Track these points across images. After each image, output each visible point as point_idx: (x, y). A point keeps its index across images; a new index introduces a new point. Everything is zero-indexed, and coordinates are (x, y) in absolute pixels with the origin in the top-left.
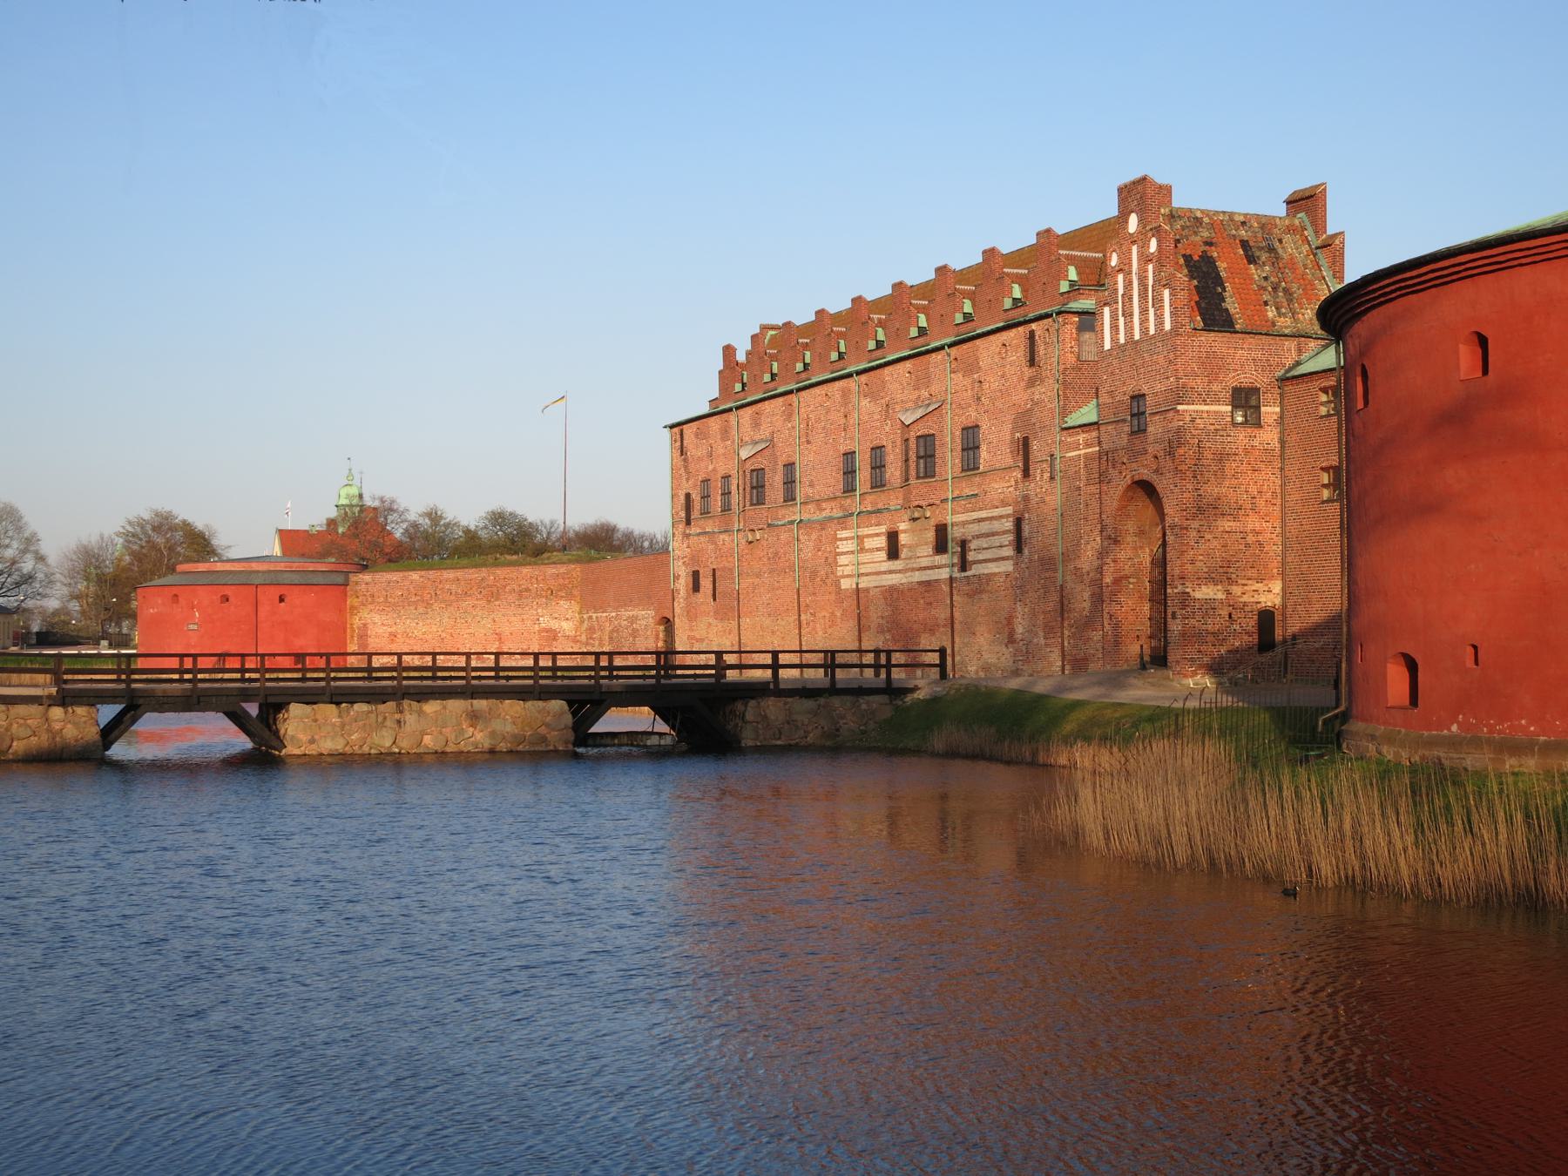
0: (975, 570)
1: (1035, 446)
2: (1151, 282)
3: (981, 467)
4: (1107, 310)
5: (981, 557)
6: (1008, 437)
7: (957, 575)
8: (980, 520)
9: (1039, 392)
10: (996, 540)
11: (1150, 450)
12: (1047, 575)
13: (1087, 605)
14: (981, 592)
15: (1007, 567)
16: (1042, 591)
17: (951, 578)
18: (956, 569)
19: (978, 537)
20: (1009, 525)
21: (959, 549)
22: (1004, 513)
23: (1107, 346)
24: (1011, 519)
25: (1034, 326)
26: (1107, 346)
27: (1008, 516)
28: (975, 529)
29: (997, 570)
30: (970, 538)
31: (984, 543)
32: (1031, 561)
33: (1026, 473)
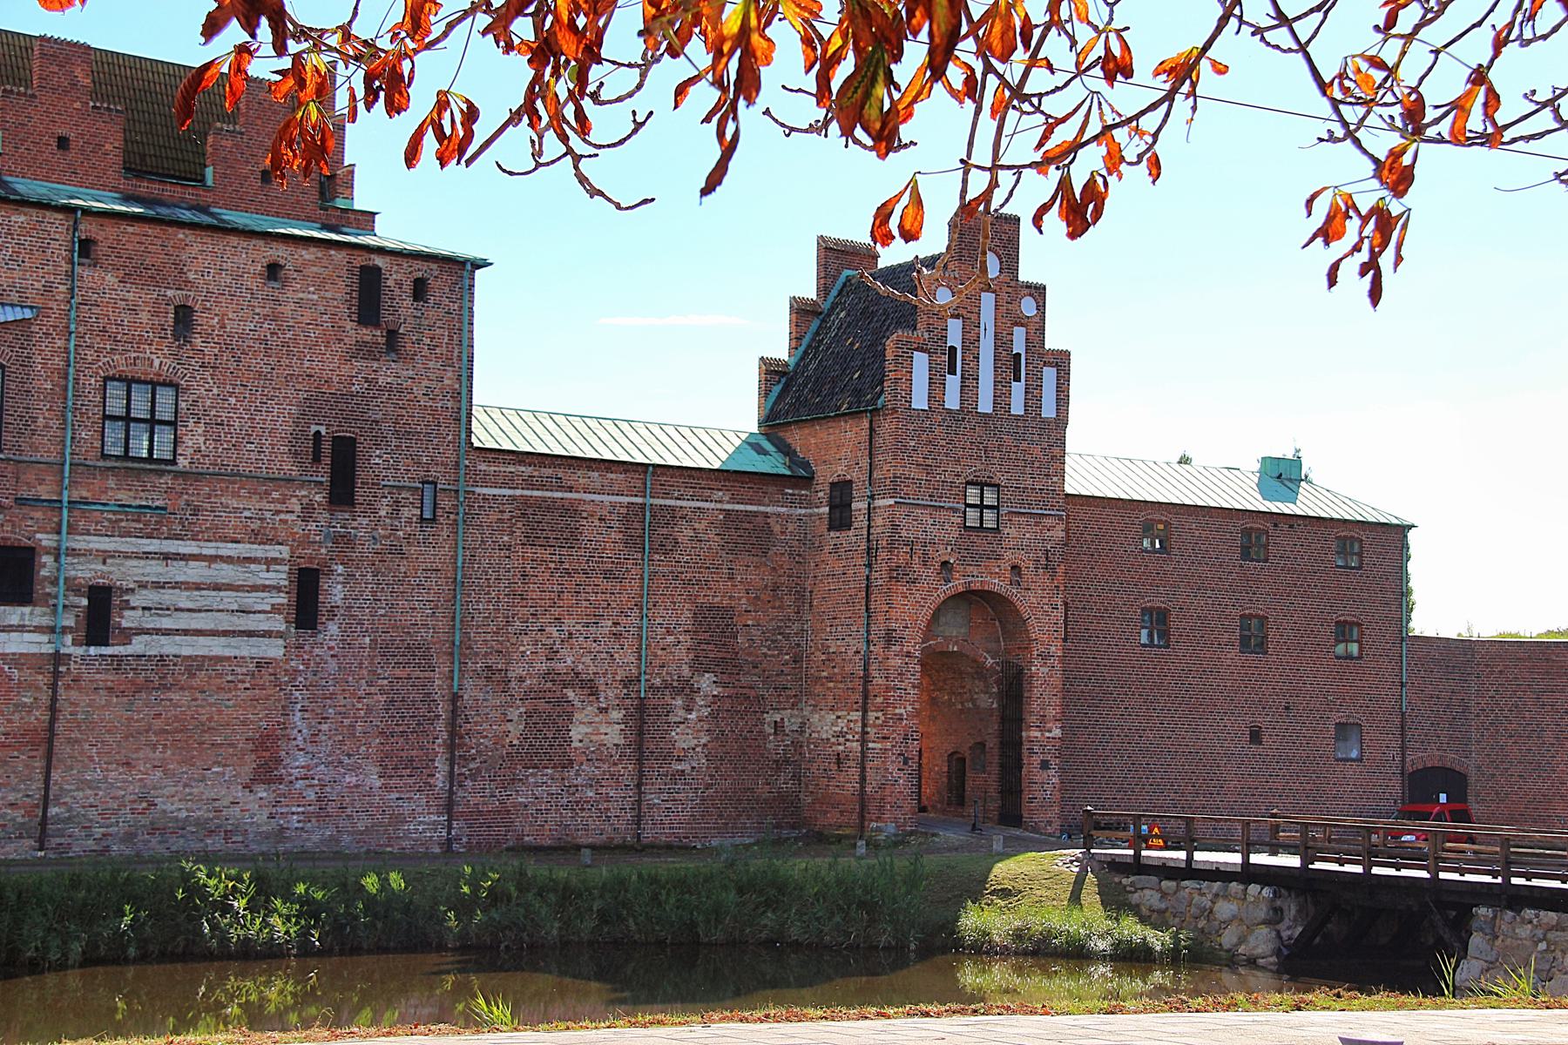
0: (138, 645)
1: (375, 461)
2: (1019, 347)
3: (182, 463)
4: (921, 361)
5: (166, 623)
6: (285, 427)
7: (68, 646)
8: (167, 557)
9: (388, 373)
10: (230, 599)
11: (1008, 555)
12: (398, 672)
13: (515, 730)
14: (165, 688)
15: (274, 650)
16: (382, 698)
17: (58, 658)
18: (69, 639)
19: (158, 586)
20: (279, 576)
21: (85, 602)
22: (260, 554)
23: (920, 401)
24: (286, 568)
25: (379, 261)
26: (920, 401)
27: (270, 562)
28: (154, 570)
29: (228, 652)
30: (131, 586)
31: (183, 599)
32: (346, 644)
33: (342, 492)
